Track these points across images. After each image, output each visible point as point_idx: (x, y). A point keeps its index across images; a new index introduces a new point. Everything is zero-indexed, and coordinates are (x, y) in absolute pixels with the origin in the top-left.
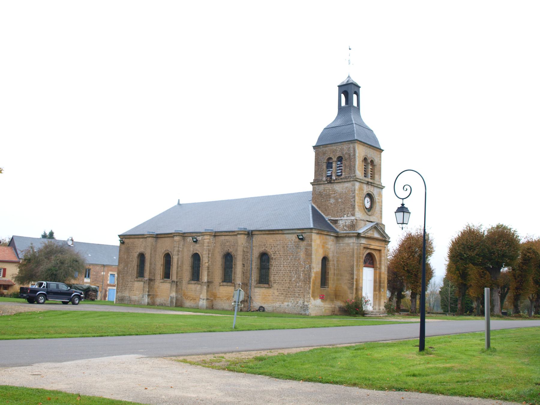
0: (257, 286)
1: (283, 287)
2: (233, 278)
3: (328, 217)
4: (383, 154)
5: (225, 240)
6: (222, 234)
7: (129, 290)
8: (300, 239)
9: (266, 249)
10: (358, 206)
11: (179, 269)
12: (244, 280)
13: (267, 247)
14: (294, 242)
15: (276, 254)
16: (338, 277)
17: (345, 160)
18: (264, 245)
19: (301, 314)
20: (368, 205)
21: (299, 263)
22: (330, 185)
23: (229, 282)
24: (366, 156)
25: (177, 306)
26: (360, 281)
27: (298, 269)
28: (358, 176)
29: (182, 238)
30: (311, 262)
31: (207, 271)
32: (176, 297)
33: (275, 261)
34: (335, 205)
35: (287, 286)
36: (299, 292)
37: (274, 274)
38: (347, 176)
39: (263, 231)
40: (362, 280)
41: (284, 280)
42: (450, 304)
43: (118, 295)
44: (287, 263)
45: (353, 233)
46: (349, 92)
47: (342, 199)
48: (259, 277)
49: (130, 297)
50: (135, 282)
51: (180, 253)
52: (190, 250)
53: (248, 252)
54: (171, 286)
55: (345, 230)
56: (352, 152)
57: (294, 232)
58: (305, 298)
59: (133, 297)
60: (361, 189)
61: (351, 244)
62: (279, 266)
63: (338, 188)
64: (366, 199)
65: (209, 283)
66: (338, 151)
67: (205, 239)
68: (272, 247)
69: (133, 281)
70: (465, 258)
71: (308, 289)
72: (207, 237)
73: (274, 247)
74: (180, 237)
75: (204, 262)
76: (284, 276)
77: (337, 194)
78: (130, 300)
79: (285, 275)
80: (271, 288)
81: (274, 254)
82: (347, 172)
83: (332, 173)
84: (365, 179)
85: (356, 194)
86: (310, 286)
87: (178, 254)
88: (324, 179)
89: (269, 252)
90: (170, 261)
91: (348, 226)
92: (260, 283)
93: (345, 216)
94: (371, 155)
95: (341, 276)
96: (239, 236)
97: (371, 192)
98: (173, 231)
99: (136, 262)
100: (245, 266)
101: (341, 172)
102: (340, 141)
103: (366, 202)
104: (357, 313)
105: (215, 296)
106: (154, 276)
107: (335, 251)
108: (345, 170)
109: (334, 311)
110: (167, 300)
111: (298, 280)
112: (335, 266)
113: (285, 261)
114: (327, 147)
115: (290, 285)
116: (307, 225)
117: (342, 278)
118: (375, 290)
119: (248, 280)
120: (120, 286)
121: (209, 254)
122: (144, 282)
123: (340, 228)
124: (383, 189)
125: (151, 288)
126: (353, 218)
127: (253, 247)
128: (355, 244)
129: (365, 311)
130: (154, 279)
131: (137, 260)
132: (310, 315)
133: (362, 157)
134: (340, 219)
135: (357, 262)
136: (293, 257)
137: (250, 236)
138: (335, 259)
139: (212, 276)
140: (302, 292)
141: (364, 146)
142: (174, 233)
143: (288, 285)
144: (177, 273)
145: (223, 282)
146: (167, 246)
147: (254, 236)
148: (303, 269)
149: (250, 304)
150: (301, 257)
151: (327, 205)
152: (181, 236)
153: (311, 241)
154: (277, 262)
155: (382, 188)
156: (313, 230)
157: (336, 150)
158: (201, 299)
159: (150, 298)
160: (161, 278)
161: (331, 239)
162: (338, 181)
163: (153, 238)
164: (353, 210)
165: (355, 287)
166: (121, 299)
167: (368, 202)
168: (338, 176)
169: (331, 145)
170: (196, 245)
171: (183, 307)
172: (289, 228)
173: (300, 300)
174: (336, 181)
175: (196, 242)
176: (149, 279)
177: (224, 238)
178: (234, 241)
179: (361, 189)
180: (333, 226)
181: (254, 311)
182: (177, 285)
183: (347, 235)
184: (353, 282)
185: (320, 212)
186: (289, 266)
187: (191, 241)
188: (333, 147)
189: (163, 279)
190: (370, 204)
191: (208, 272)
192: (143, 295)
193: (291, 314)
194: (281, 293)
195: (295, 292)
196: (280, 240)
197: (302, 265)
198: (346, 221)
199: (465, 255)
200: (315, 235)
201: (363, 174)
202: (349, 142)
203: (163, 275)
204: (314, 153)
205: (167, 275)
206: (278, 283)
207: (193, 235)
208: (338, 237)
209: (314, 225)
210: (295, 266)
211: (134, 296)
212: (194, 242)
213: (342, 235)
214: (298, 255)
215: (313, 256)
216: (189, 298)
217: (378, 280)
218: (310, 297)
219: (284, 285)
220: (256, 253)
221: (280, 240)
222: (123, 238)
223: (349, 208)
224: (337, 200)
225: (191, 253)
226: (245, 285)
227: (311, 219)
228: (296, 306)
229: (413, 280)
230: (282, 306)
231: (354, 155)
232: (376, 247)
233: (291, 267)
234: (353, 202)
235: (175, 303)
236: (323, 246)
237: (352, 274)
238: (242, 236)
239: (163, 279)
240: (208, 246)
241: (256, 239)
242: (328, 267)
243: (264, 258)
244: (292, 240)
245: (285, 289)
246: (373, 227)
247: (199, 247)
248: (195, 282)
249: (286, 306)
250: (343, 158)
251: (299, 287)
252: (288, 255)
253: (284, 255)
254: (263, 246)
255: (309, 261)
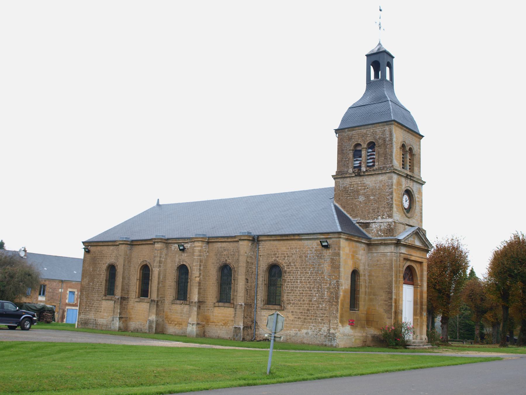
0: (264, 307)
1: (300, 309)
2: (232, 297)
3: (356, 219)
4: (422, 141)
5: (221, 247)
6: (218, 240)
7: (94, 311)
8: (323, 246)
9: (277, 259)
10: (396, 205)
11: (161, 285)
12: (247, 300)
13: (278, 257)
14: (315, 251)
15: (291, 265)
16: (370, 297)
17: (379, 146)
18: (274, 255)
19: (326, 345)
20: (406, 205)
21: (322, 278)
22: (358, 178)
23: (227, 302)
24: (404, 142)
25: (157, 332)
26: (400, 302)
27: (321, 285)
28: (396, 167)
29: (165, 245)
30: (339, 277)
31: (198, 287)
32: (157, 321)
33: (289, 275)
34: (366, 203)
35: (306, 308)
36: (323, 316)
37: (288, 293)
38: (381, 166)
39: (273, 237)
40: (402, 301)
41: (302, 299)
42: (459, 329)
43: (81, 317)
44: (305, 277)
45: (391, 240)
46: (381, 62)
47: (375, 196)
48: (267, 296)
49: (95, 320)
50: (103, 301)
51: (161, 265)
52: (175, 261)
53: (252, 264)
54: (150, 307)
55: (380, 236)
56: (387, 136)
57: (316, 237)
58: (331, 324)
59: (100, 319)
60: (399, 184)
61: (389, 254)
62: (294, 282)
63: (370, 181)
64: (404, 197)
65: (201, 303)
66: (370, 134)
67: (195, 247)
68: (285, 257)
69: (100, 299)
70: (516, 275)
71: (334, 313)
72: (198, 244)
73: (288, 256)
74: (162, 244)
75: (193, 277)
76: (301, 295)
77: (368, 190)
78: (95, 324)
79: (303, 293)
80: (284, 310)
81: (288, 266)
82: (381, 162)
83: (360, 163)
84: (403, 170)
85: (394, 189)
86: (337, 308)
87: (160, 266)
88: (351, 171)
89: (281, 263)
90: (149, 274)
91: (384, 231)
92: (268, 304)
93: (380, 217)
94: (410, 141)
95: (374, 295)
96: (241, 243)
97: (410, 187)
98: (153, 237)
99: (105, 276)
100: (249, 281)
101: (374, 162)
102: (371, 122)
103: (404, 201)
104: (397, 345)
105: (207, 320)
106: (128, 293)
107: (367, 263)
108: (378, 159)
109: (366, 342)
110: (144, 325)
111: (321, 300)
112: (367, 282)
113: (304, 275)
114: (353, 130)
115: (309, 307)
116: (333, 229)
117: (376, 298)
118: (415, 314)
119: (252, 299)
120: (83, 305)
121: (200, 266)
122: (115, 302)
123: (373, 233)
124: (423, 185)
125: (123, 308)
126: (390, 220)
127: (259, 257)
128: (393, 254)
129: (407, 341)
130: (128, 298)
131: (105, 273)
132: (338, 347)
133: (400, 143)
134: (372, 221)
135: (396, 277)
136: (314, 270)
137: (255, 243)
138: (367, 274)
139: (204, 295)
140: (327, 316)
141: (402, 129)
142: (155, 239)
143: (306, 307)
144: (158, 290)
145: (218, 302)
146: (145, 256)
147: (261, 242)
148: (328, 285)
149: (255, 331)
150: (325, 270)
151: (355, 204)
152: (164, 242)
153: (339, 250)
154: (292, 277)
155: (422, 183)
156: (342, 234)
157: (366, 134)
158: (190, 324)
159: (121, 321)
160: (137, 297)
161: (362, 247)
162: (368, 174)
163: (126, 246)
164: (391, 210)
165: (393, 310)
166: (84, 323)
167: (406, 201)
168: (368, 166)
169: (359, 128)
170: (183, 255)
171: (165, 334)
172: (309, 232)
173: (323, 327)
174: (366, 174)
175: (183, 250)
176: (121, 298)
177: (220, 245)
178: (233, 250)
179: (399, 184)
180: (364, 231)
181: (261, 340)
182: (157, 305)
183: (383, 242)
184: (392, 303)
185: (345, 212)
186: (309, 282)
187: (176, 250)
188: (362, 131)
189: (138, 297)
190: (408, 204)
191: (199, 289)
192: (113, 318)
193: (312, 344)
194: (297, 317)
195: (317, 316)
196: (296, 248)
197: (327, 280)
198: (381, 224)
199: (516, 271)
200: (344, 241)
201: (401, 164)
202: (383, 124)
203: (139, 293)
204: (336, 140)
205: (144, 292)
206: (293, 304)
207: (180, 242)
208: (370, 245)
209: (342, 229)
210: (317, 282)
211: (101, 318)
212: (180, 250)
213: (377, 242)
214: (321, 268)
215: (342, 269)
216: (172, 323)
217: (419, 301)
218: (337, 323)
219: (301, 306)
220: (263, 265)
221: (296, 248)
222: (88, 246)
223: (385, 207)
224: (368, 197)
225: (176, 265)
226: (249, 306)
227: (337, 221)
228: (319, 334)
229: (444, 302)
230: (299, 335)
231: (391, 140)
232: (417, 258)
233: (311, 283)
234: (390, 200)
235: (154, 329)
236: (353, 256)
237: (390, 293)
238: (246, 243)
239: (138, 297)
240: (200, 256)
241: (264, 246)
242: (358, 283)
243: (274, 270)
244: (313, 248)
245: (304, 312)
246: (414, 233)
247: (187, 256)
248: (182, 301)
249: (304, 335)
250: (376, 143)
251: (322, 309)
252: (307, 268)
253: (301, 267)
254: (273, 256)
255: (336, 275)
